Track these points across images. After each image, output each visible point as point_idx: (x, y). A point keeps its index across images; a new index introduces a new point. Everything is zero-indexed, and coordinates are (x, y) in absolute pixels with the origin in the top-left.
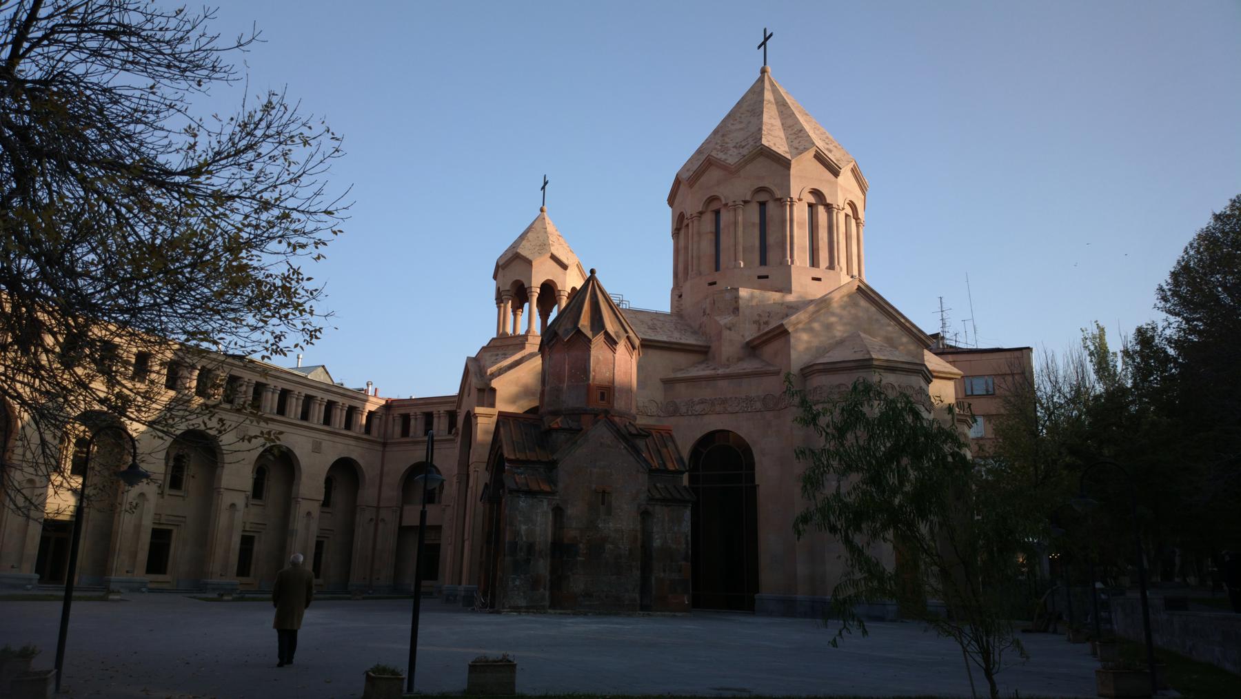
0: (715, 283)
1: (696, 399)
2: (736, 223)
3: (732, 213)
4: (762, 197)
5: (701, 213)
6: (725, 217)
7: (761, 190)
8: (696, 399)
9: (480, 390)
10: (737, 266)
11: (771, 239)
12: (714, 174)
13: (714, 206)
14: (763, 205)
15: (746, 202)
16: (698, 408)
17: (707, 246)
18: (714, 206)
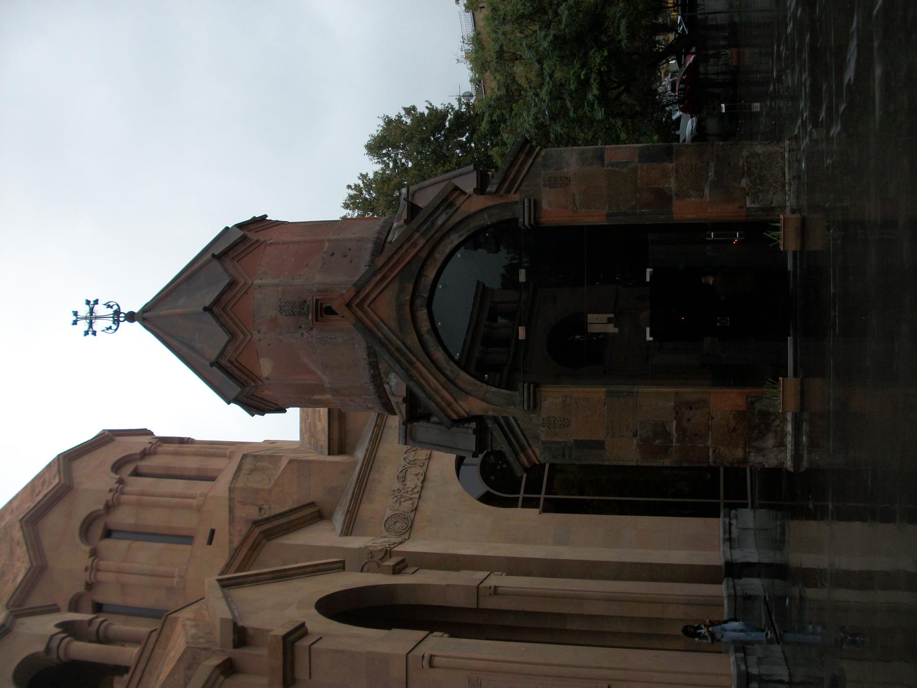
0: (213, 532)
1: (397, 485)
2: (143, 494)
3: (124, 498)
4: (130, 468)
5: (94, 553)
6: (123, 518)
7: (117, 467)
8: (397, 485)
9: (229, 668)
10: (205, 496)
11: (191, 464)
12: (55, 520)
13: (98, 530)
14: (136, 473)
15: (121, 481)
16: (412, 482)
17: (146, 556)
18: (98, 530)
